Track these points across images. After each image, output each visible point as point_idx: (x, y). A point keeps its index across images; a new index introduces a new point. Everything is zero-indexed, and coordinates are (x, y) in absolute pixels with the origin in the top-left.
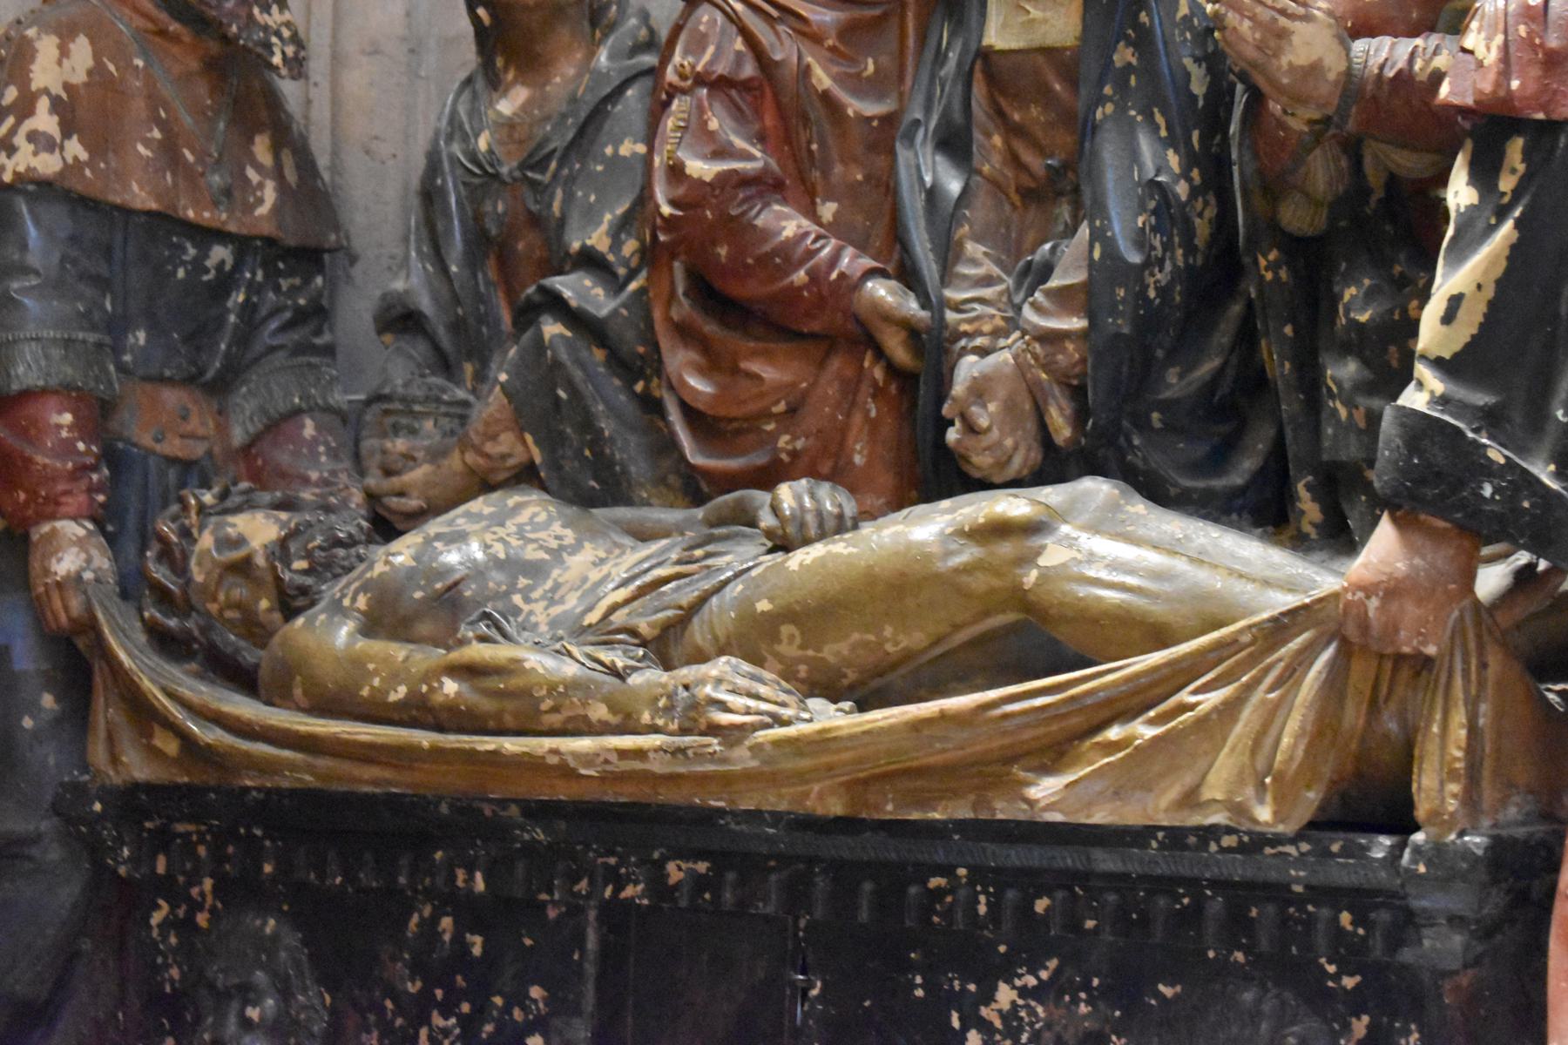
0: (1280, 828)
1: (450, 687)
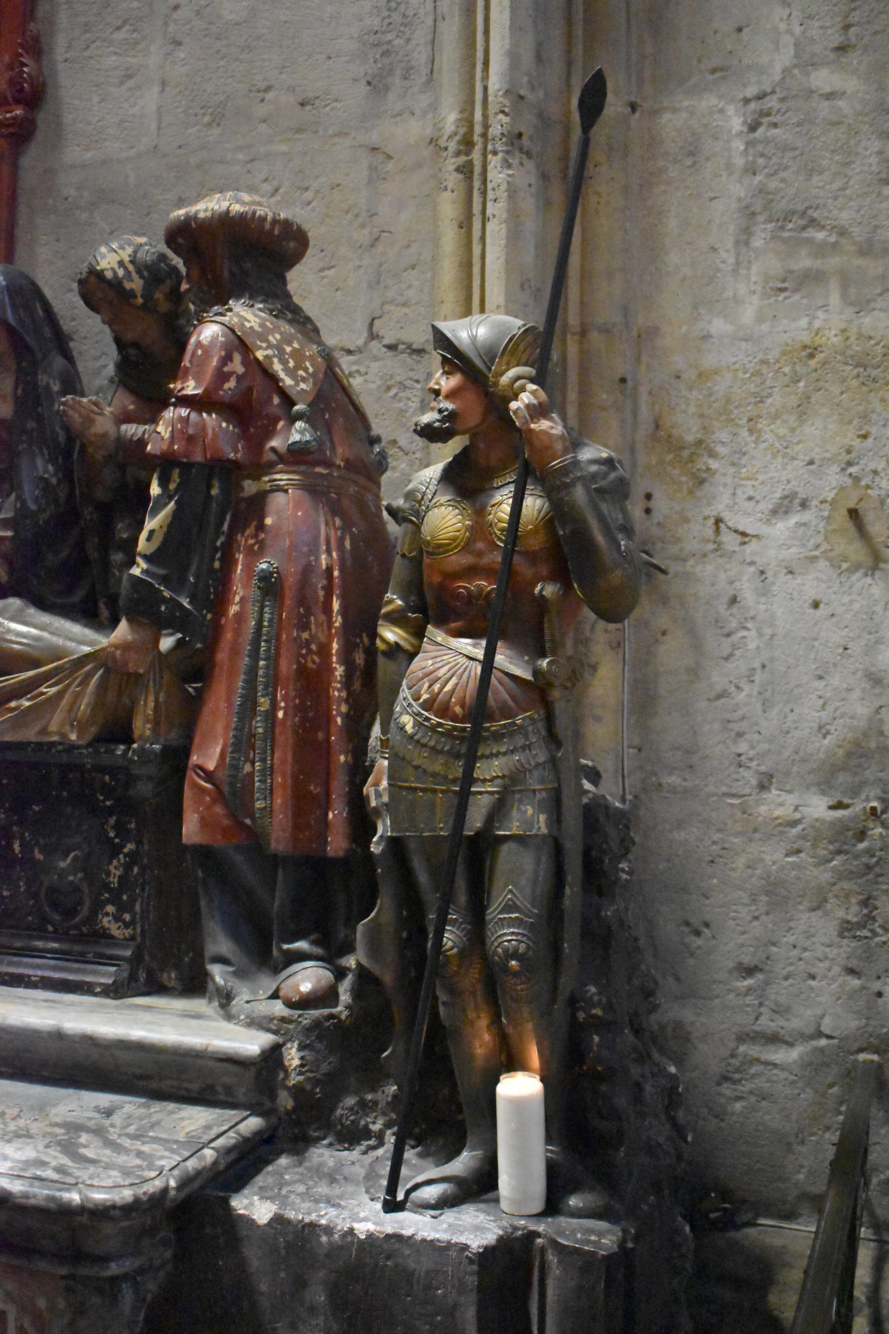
0: (80, 742)
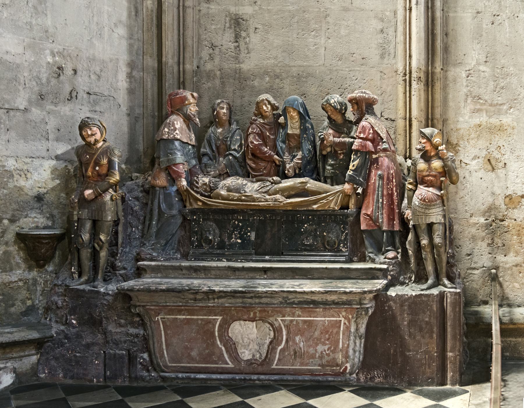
1: (243, 198)
